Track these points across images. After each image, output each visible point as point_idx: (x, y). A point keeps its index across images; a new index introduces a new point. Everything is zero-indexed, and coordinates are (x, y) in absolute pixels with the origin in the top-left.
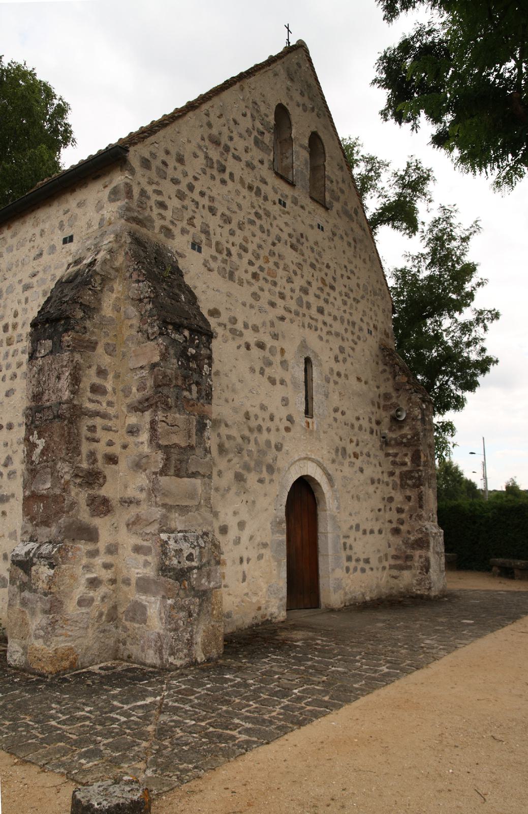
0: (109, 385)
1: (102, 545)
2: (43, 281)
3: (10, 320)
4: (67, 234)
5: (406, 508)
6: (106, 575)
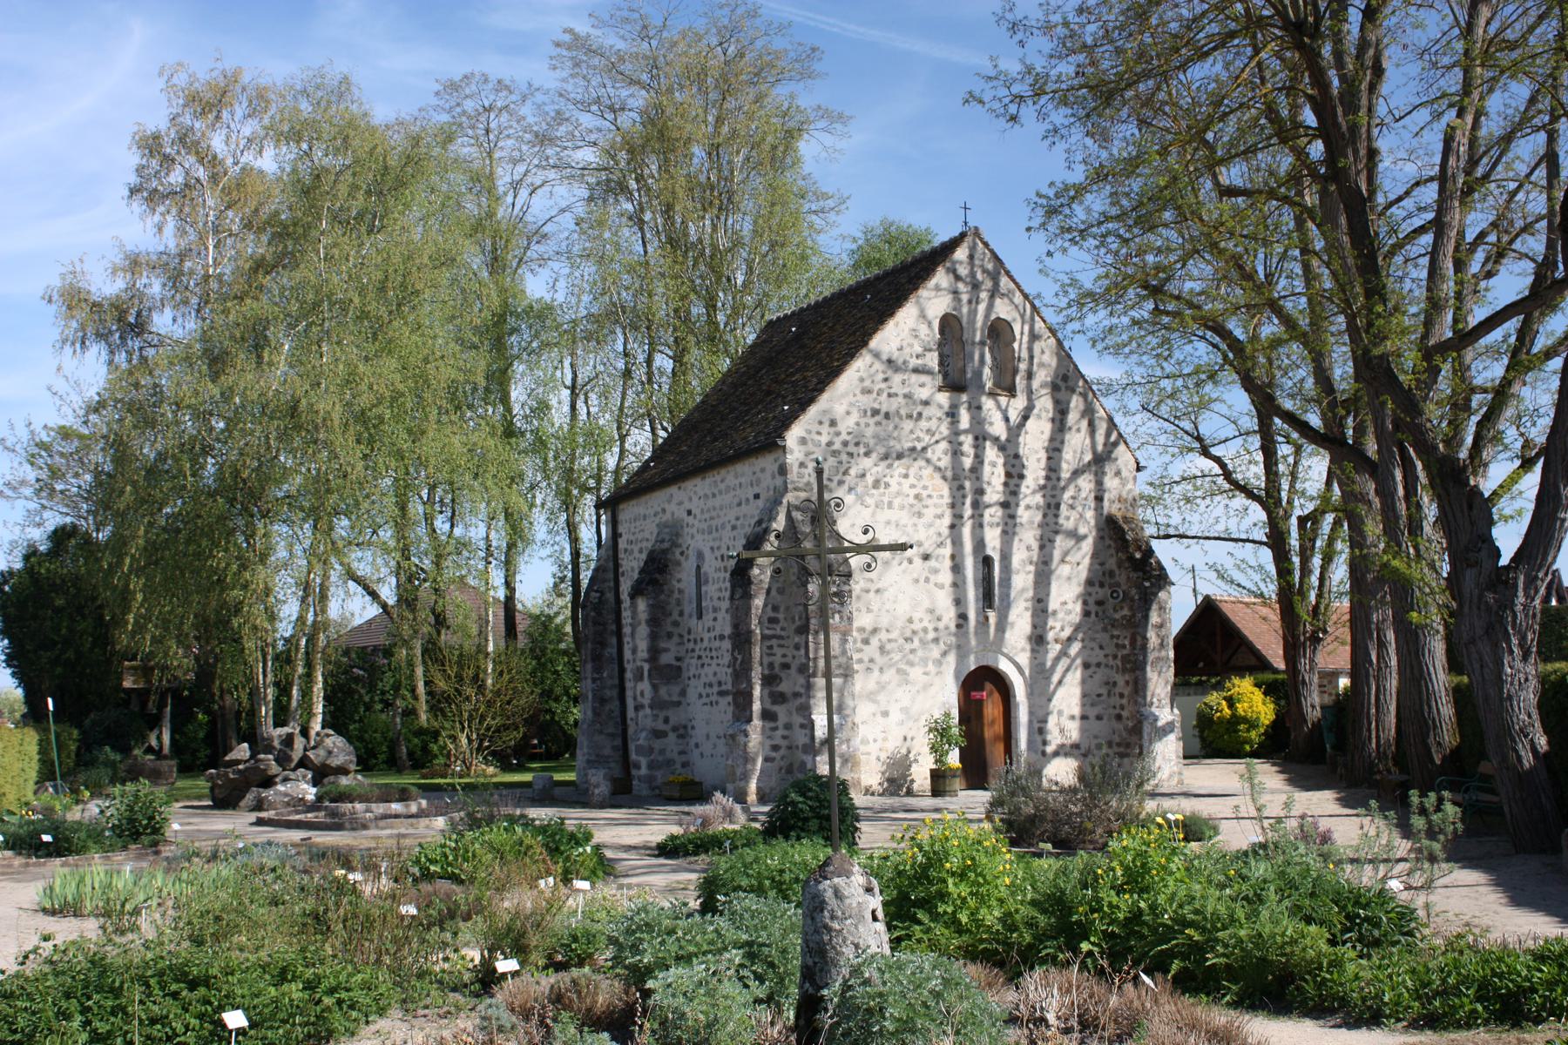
0: (781, 616)
1: (780, 723)
2: (743, 526)
3: (724, 551)
4: (757, 490)
5: (1126, 693)
6: (784, 743)
